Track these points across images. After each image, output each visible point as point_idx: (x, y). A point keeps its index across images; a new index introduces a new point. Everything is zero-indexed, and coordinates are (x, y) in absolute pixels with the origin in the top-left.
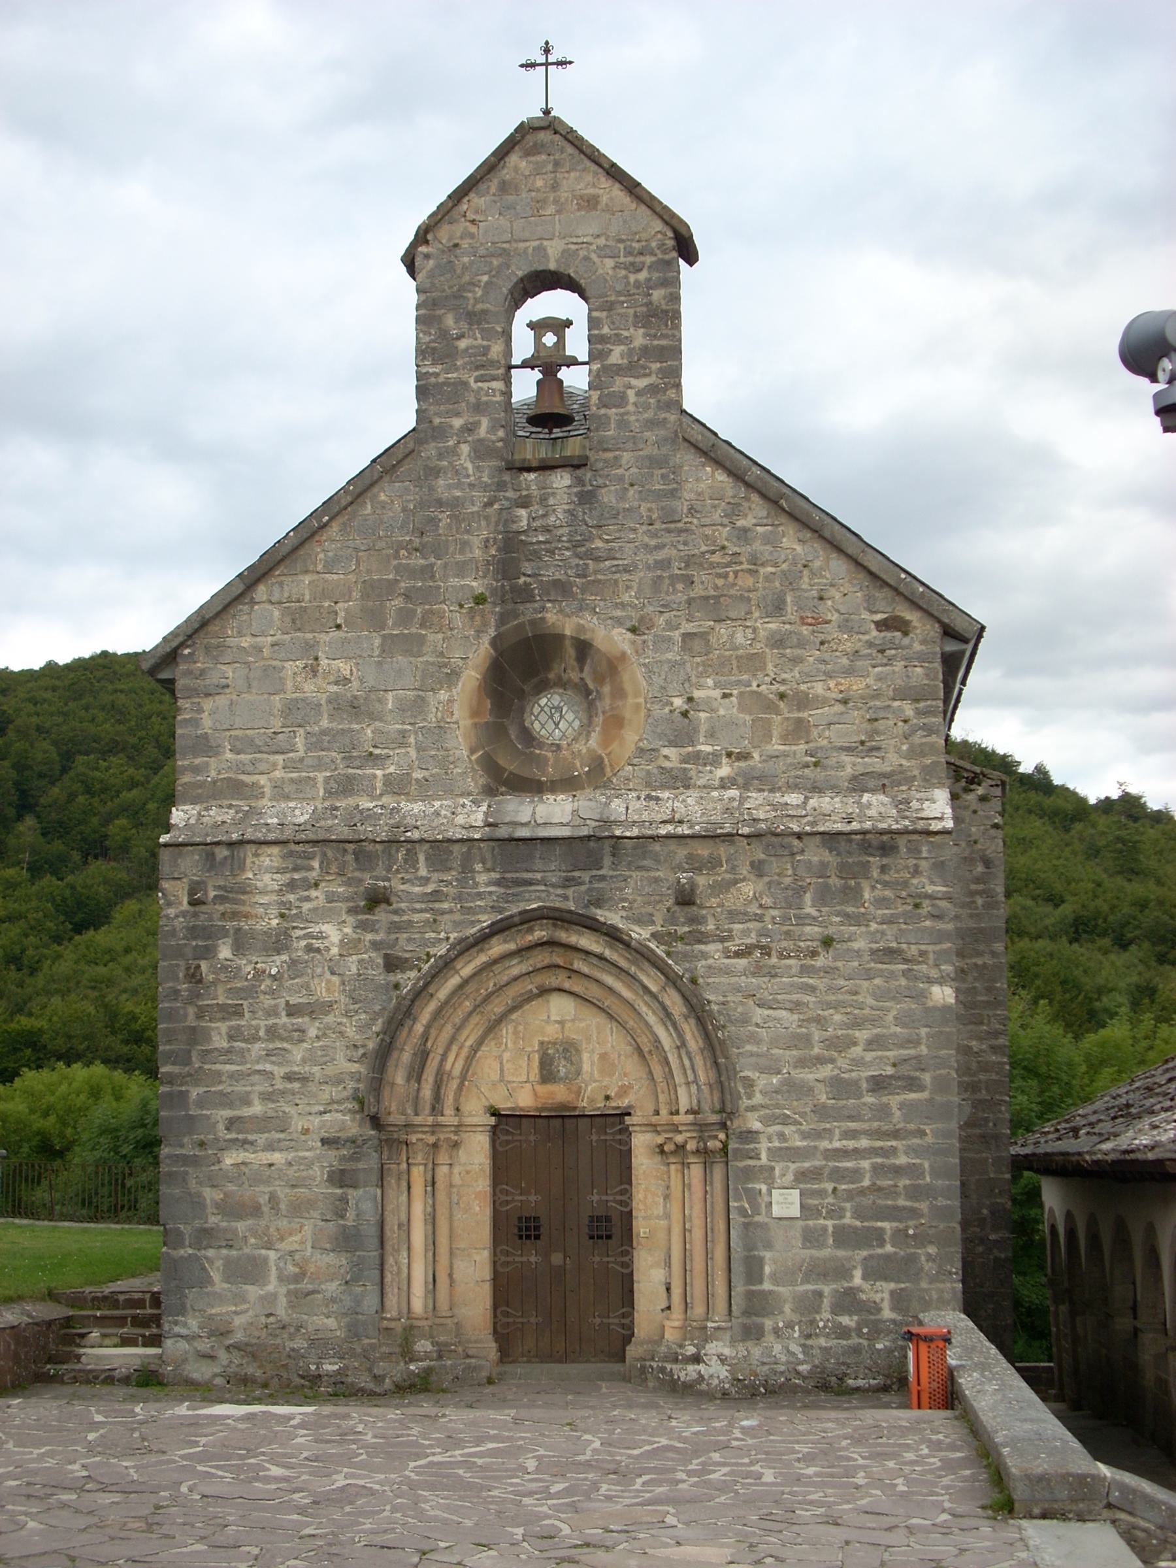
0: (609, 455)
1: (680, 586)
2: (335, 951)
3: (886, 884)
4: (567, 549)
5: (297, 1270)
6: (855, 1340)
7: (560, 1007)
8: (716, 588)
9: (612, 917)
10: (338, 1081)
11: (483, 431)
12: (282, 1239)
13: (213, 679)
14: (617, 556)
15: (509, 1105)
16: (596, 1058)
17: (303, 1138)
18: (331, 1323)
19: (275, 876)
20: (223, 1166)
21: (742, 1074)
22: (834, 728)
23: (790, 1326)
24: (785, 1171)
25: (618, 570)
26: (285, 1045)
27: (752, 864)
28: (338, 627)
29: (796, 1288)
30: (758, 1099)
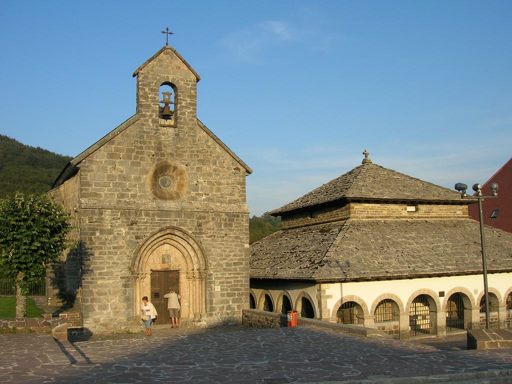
0: (182, 126)
2: (124, 234)
3: (237, 223)
9: (184, 228)
10: (125, 264)
11: (154, 117)
13: (90, 168)
18: (123, 318)
22: (226, 190)
24: (218, 282)
25: (183, 152)
28: (120, 158)
30: (212, 267)
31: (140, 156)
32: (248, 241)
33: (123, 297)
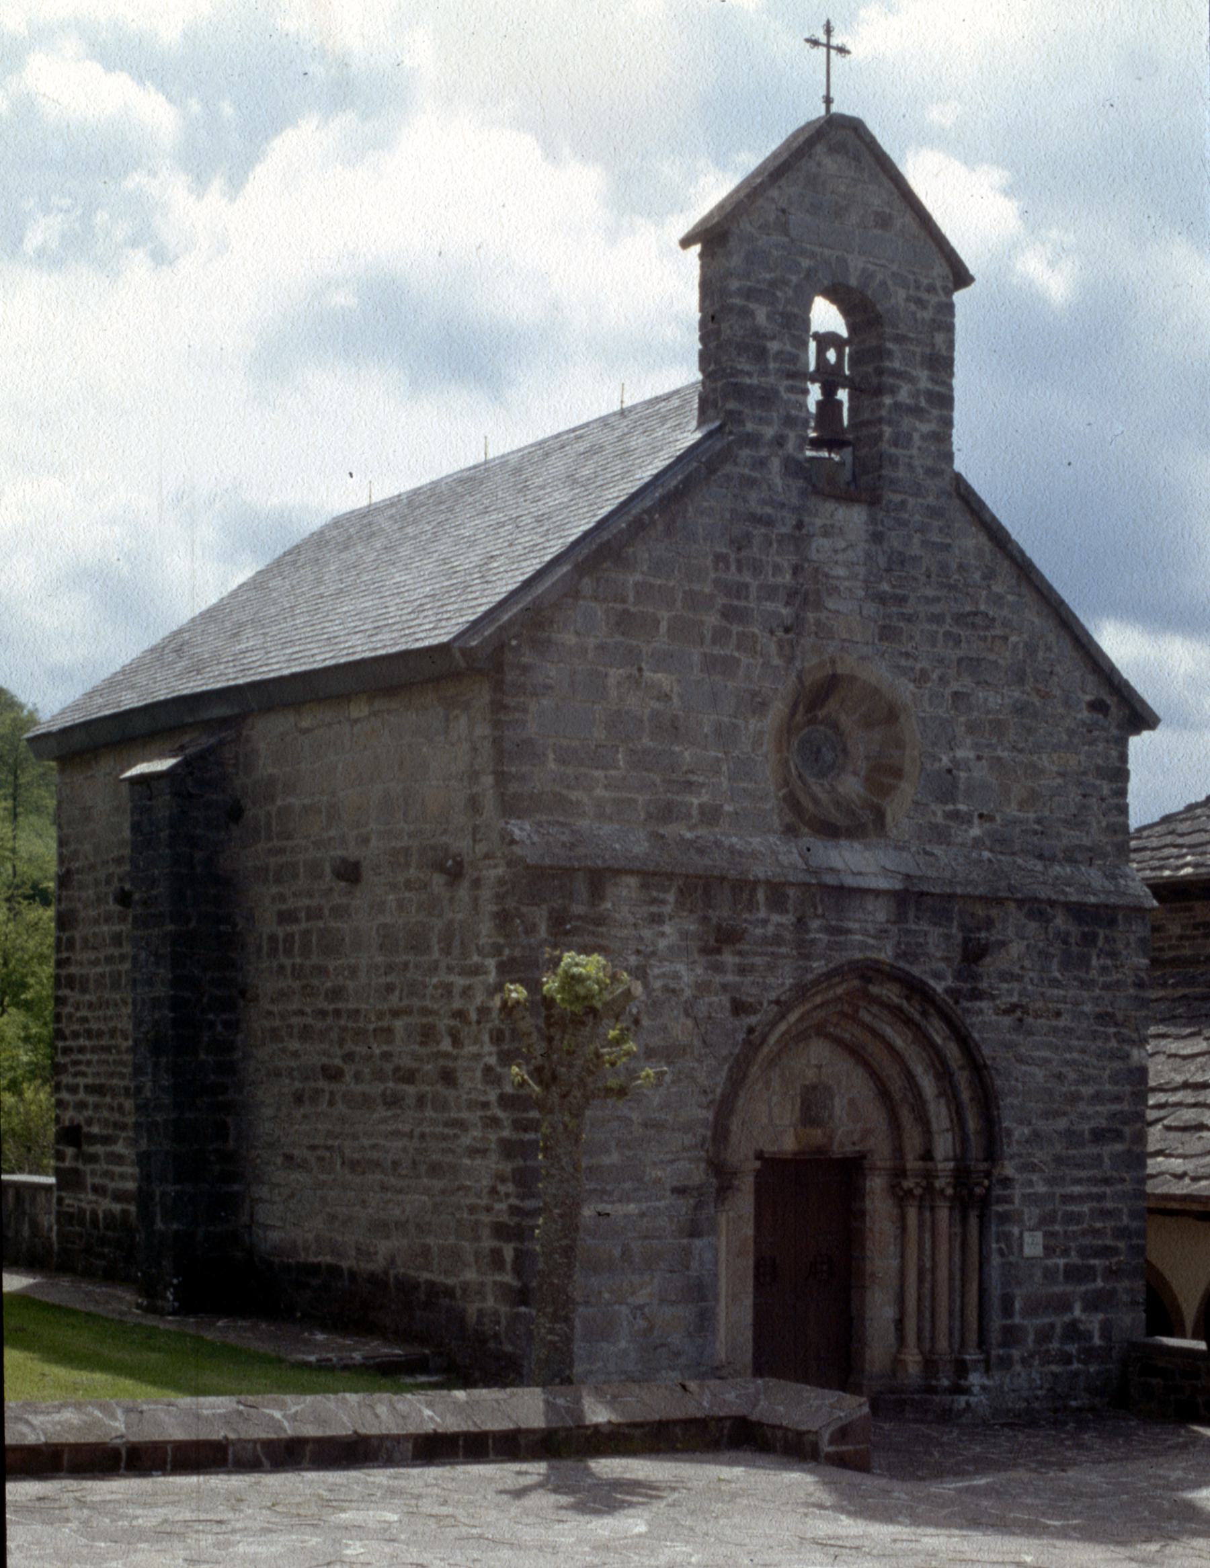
0: (897, 498)
6: (1075, 1366)
7: (818, 1051)
12: (633, 1293)
16: (845, 1101)
23: (1031, 1356)
24: (1031, 1214)
30: (1015, 1148)
31: (736, 628)
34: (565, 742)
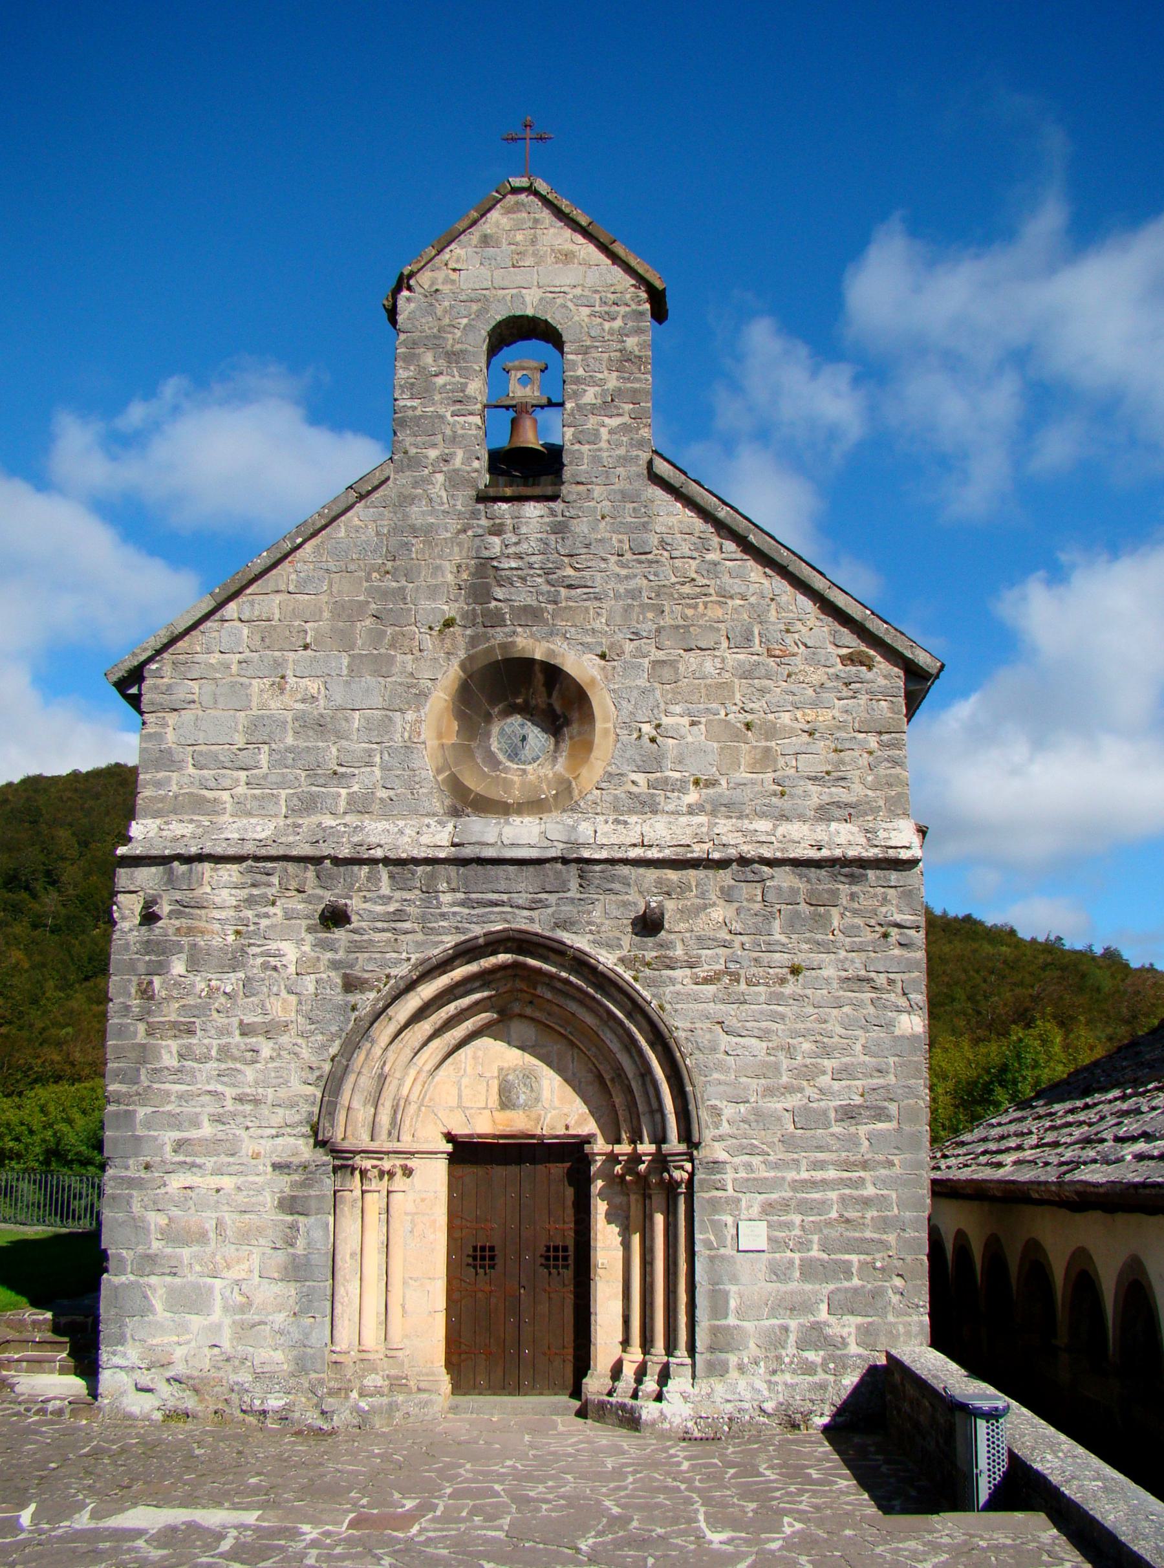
1: (650, 615)
2: (292, 969)
3: (855, 912)
4: (539, 576)
5: (244, 1300)
6: (820, 1376)
8: (685, 618)
9: (579, 942)
11: (458, 461)
12: (228, 1267)
14: (589, 584)
15: (467, 1132)
17: (254, 1162)
19: (233, 891)
20: (168, 1189)
21: (709, 1103)
24: (752, 1203)
26: (238, 1066)
27: (722, 889)
29: (762, 1322)
30: (725, 1128)
32: (919, 998)
33: (280, 1257)
34: (203, 748)
